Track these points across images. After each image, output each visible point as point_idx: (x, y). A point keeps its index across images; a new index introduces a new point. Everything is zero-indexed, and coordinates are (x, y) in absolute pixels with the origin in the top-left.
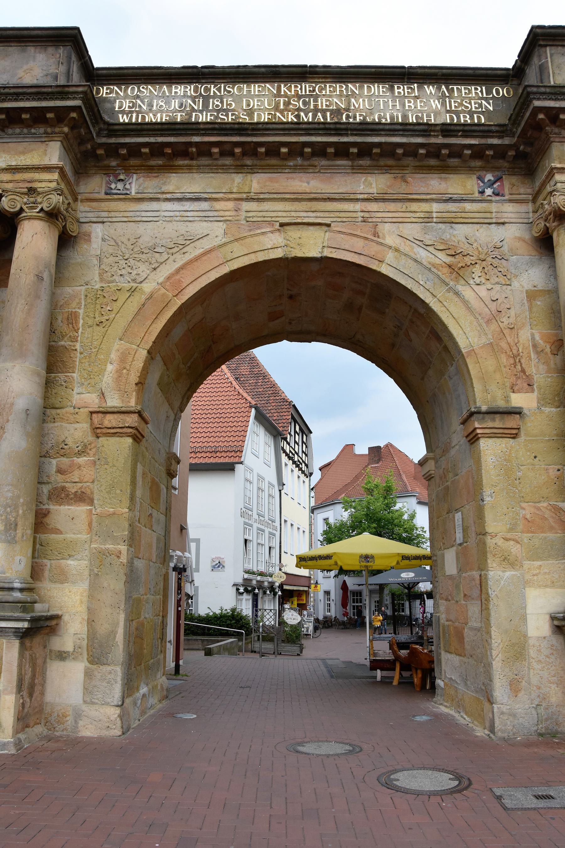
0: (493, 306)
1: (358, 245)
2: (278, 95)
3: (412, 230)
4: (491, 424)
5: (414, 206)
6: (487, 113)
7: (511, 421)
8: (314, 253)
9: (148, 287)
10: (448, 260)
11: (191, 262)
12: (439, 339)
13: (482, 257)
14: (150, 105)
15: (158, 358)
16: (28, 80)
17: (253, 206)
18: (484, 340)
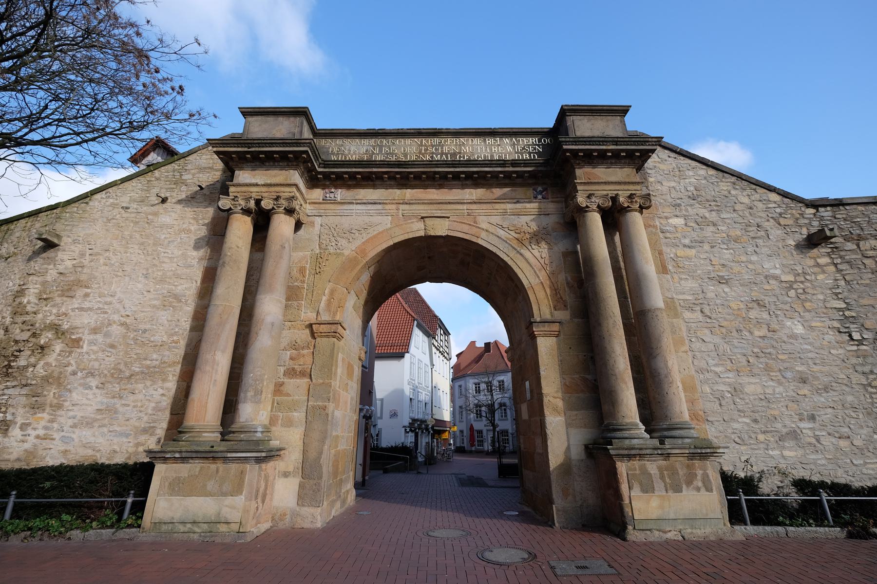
1: (466, 228)
2: (422, 145)
3: (496, 219)
4: (542, 329)
6: (539, 153)
9: (347, 252)
10: (516, 236)
12: (512, 280)
15: (352, 292)
16: (278, 135)
17: (406, 207)
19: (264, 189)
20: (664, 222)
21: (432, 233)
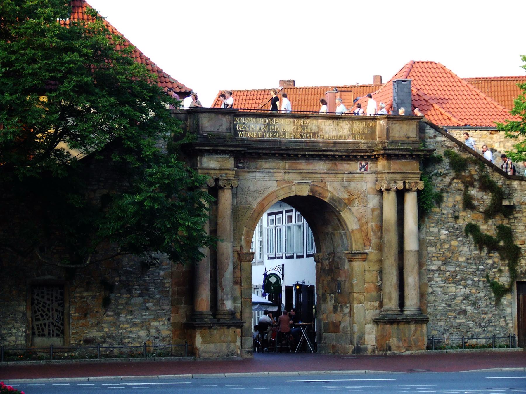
5: (338, 176)
7: (364, 256)
11: (266, 197)
14: (249, 128)
19: (218, 172)
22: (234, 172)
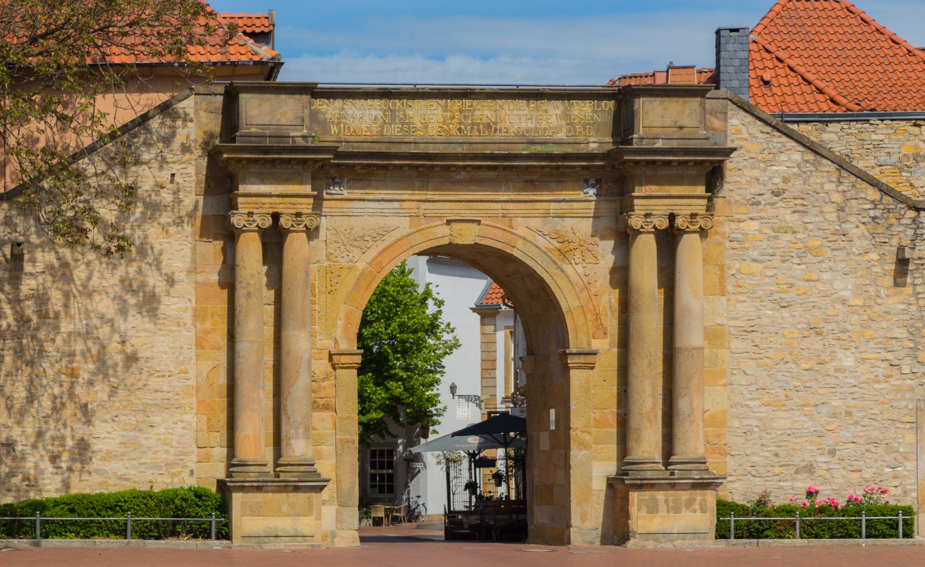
0: (585, 279)
1: (499, 234)
5: (538, 205)
7: (589, 359)
8: (469, 241)
9: (361, 266)
10: (559, 246)
11: (388, 248)
13: (582, 243)
18: (577, 303)
20: (733, 226)
21: (458, 241)
22: (311, 201)
